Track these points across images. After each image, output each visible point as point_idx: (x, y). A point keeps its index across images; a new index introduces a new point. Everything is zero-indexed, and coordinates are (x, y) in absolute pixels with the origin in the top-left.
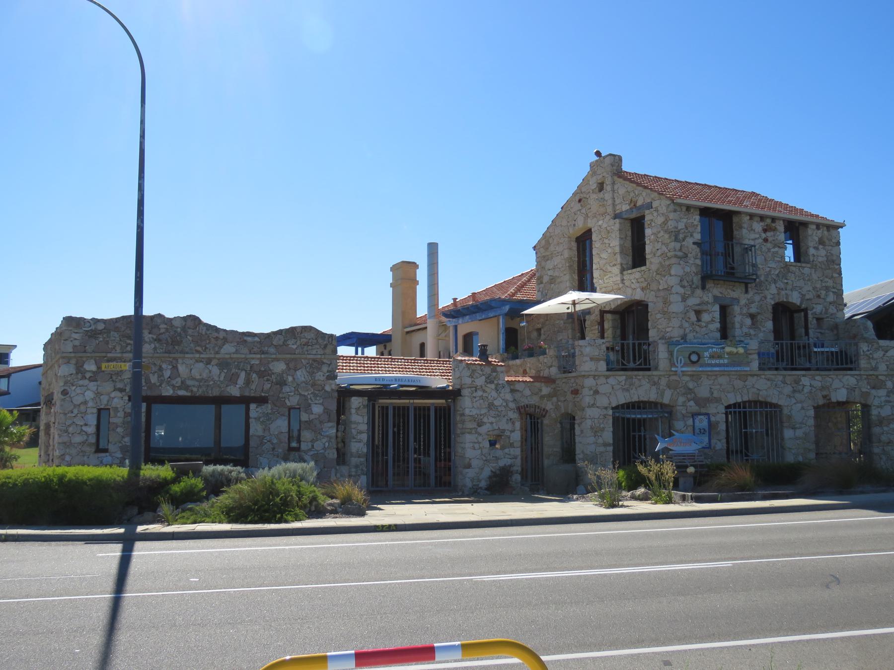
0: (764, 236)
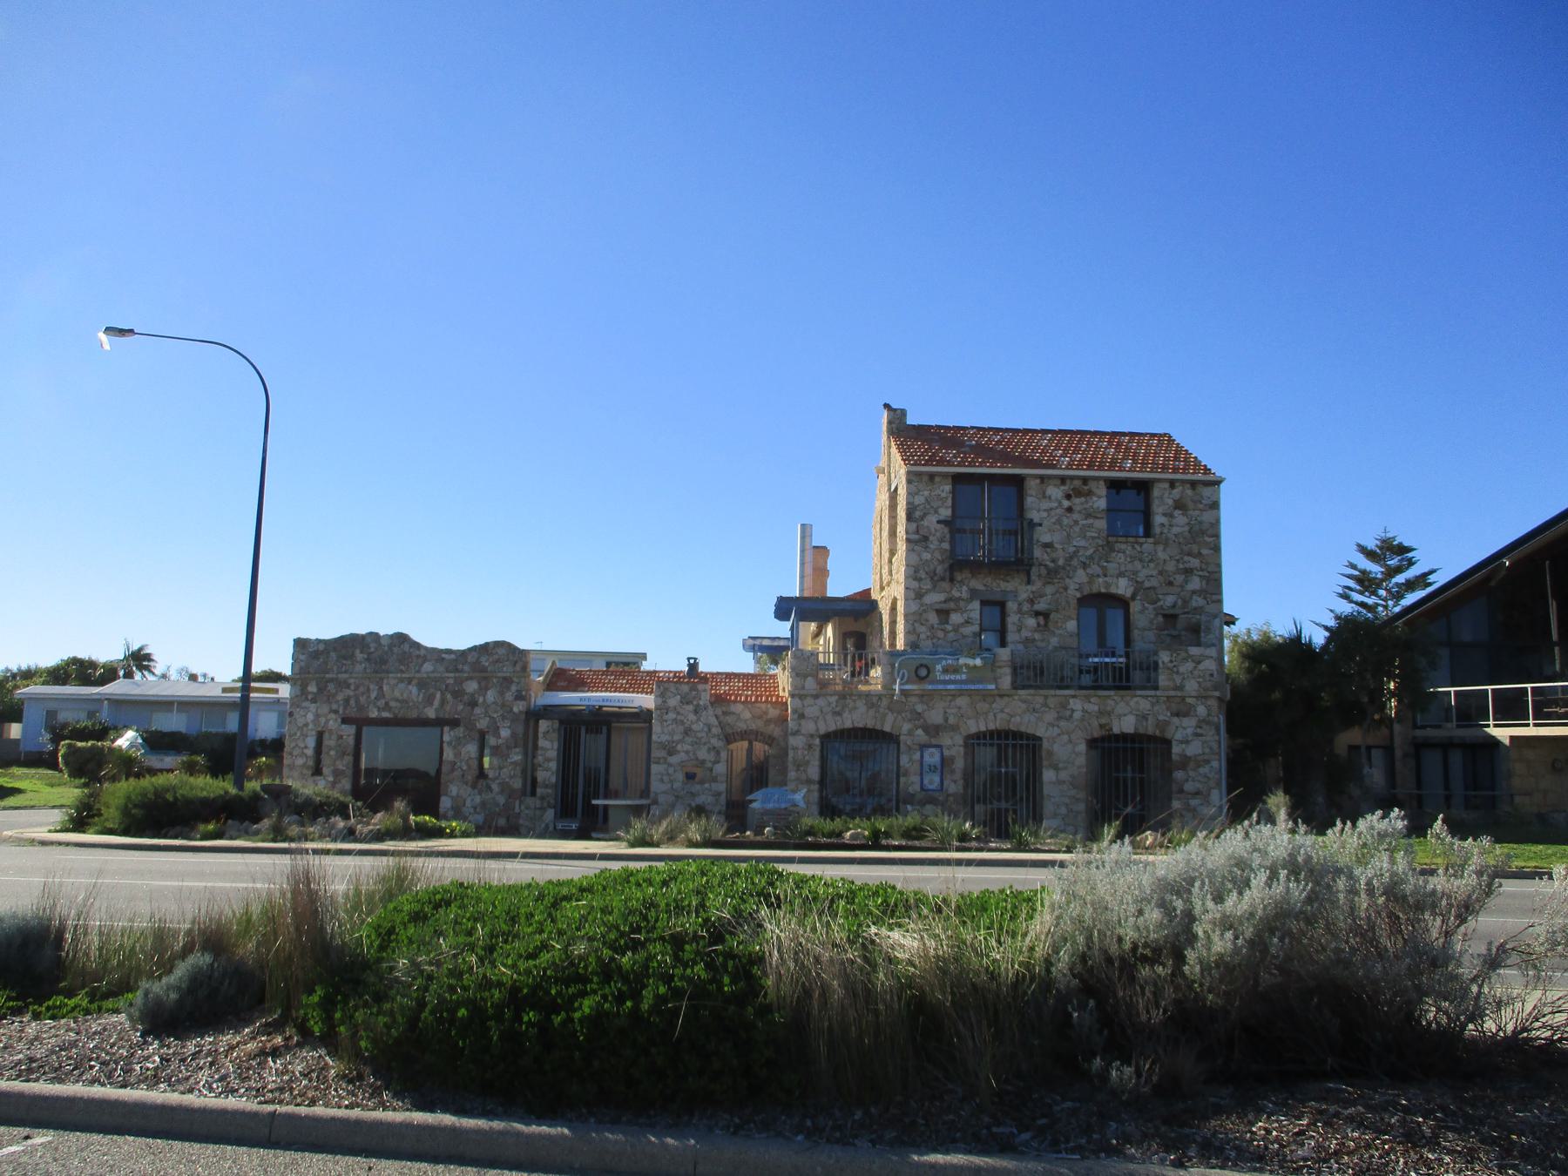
0: (1066, 503)
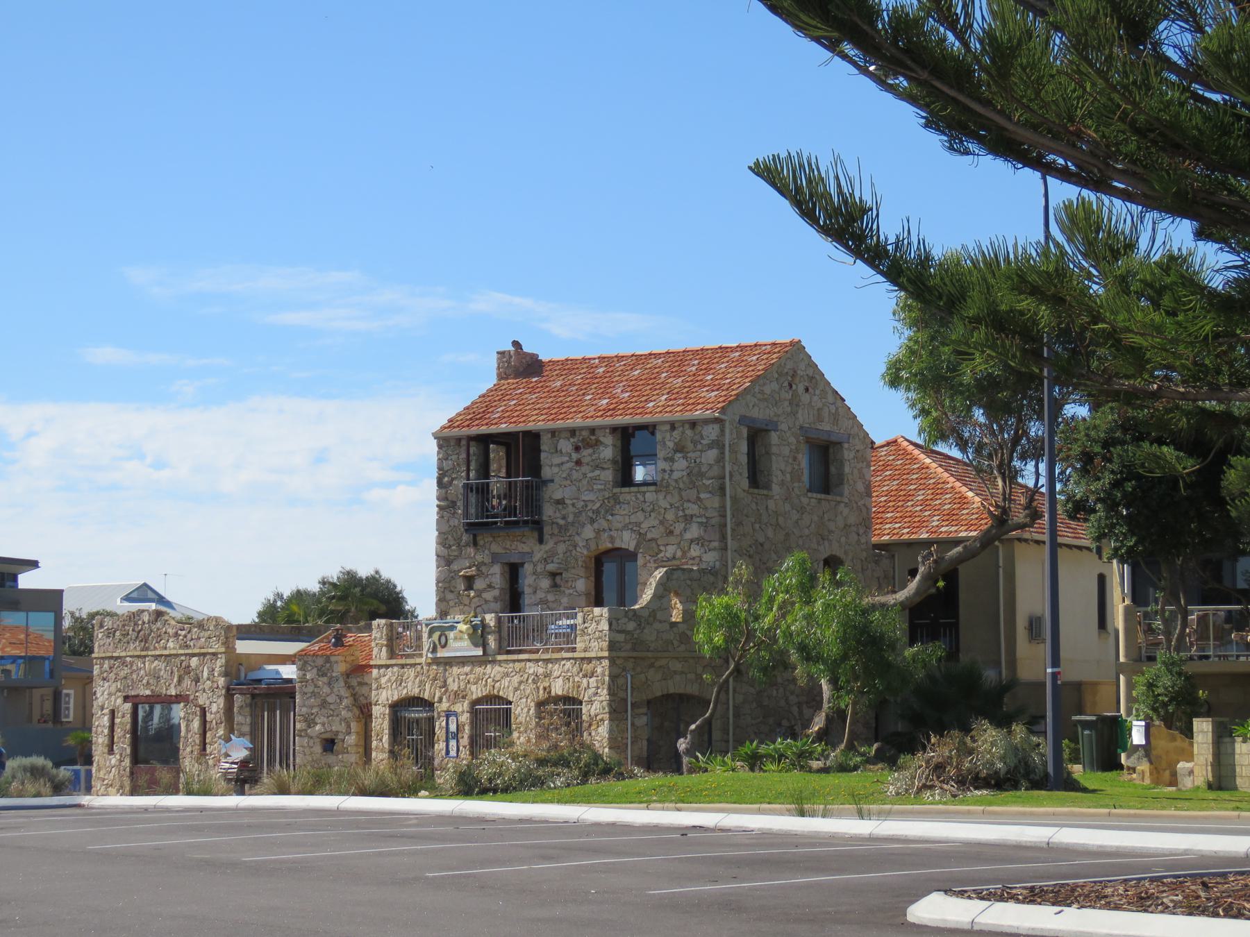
0: (575, 456)
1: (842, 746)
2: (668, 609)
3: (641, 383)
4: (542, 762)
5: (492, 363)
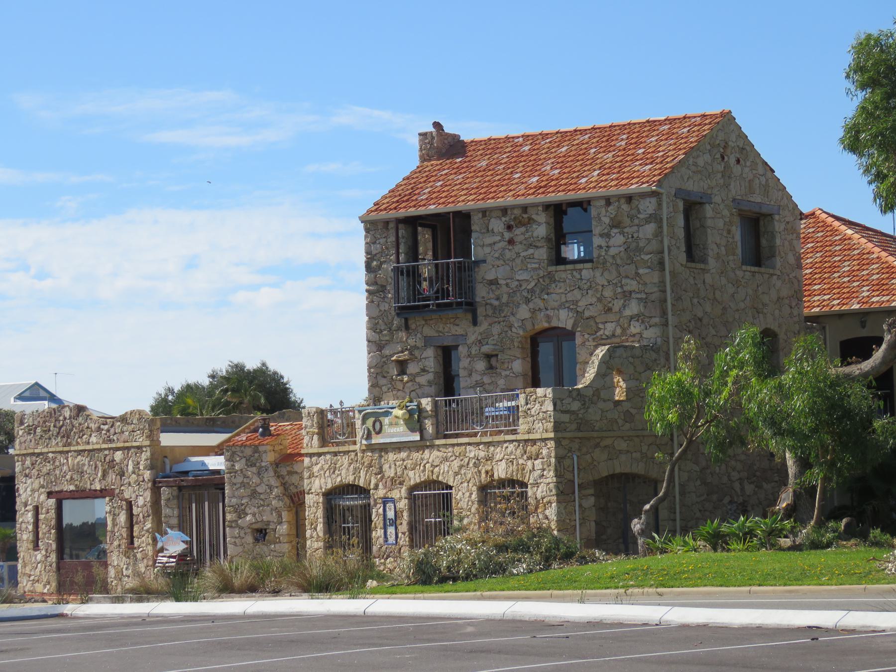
0: (507, 235)
1: (812, 523)
2: (612, 387)
3: (570, 159)
4: (502, 548)
5: (415, 142)
